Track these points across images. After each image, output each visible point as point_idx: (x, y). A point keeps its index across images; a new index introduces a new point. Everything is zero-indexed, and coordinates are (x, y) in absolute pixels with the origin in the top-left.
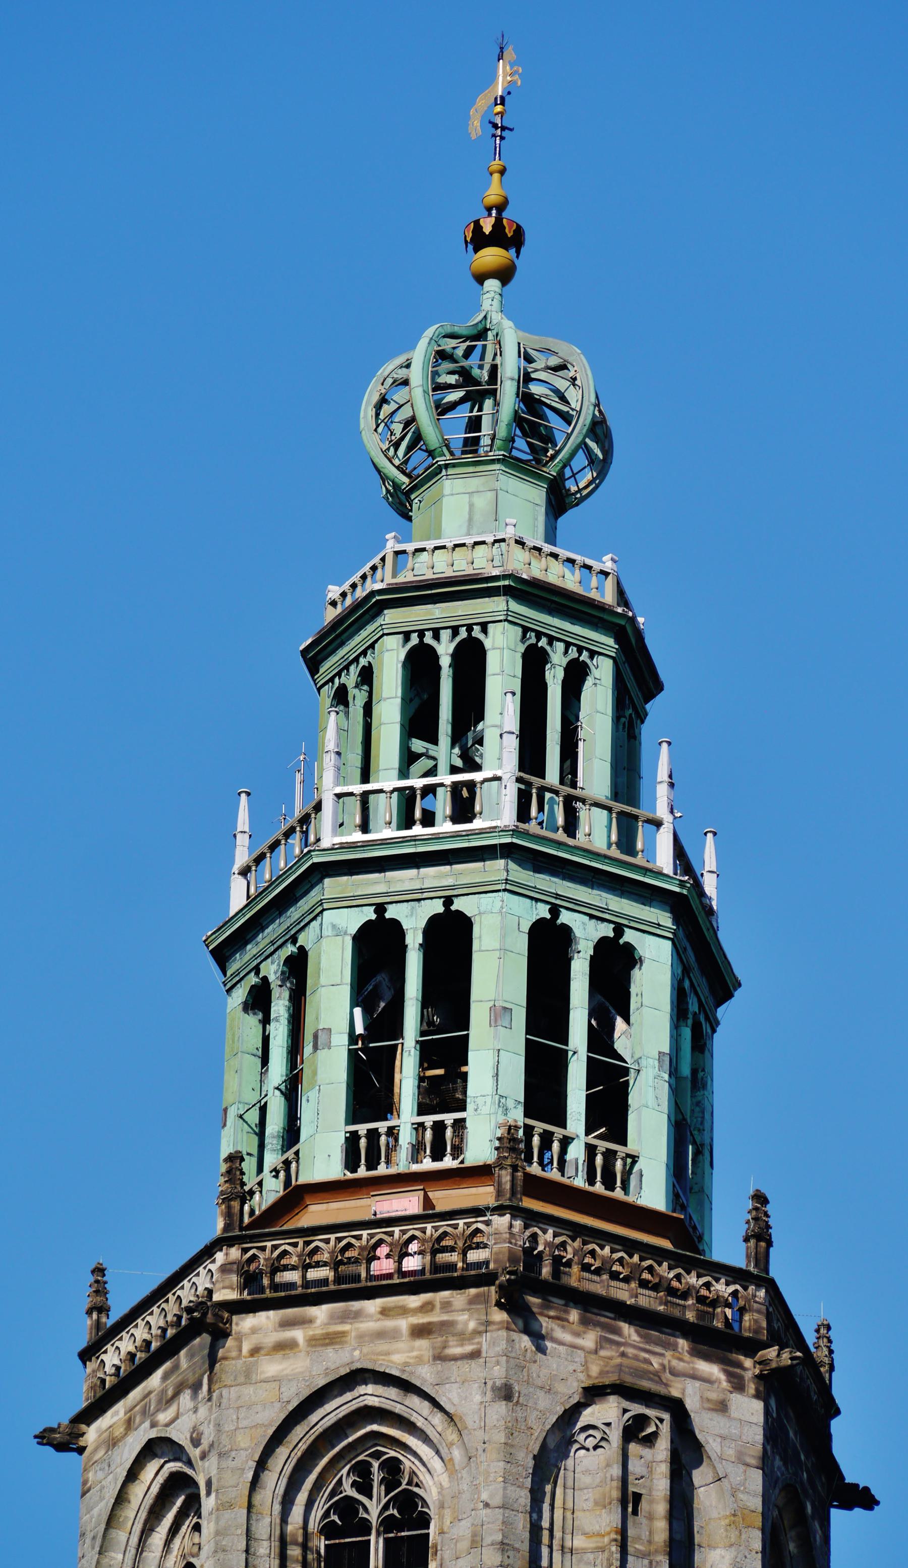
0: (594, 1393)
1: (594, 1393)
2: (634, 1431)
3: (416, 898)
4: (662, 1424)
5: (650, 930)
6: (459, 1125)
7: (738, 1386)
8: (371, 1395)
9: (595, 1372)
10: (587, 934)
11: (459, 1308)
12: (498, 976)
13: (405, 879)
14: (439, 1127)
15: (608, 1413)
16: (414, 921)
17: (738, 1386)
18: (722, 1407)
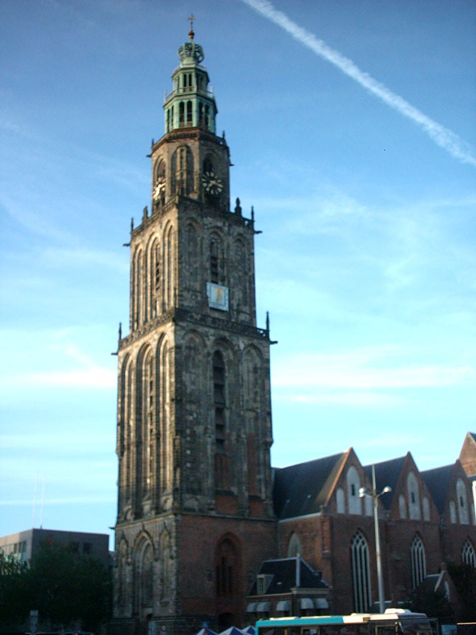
0: (177, 148)
1: (177, 148)
2: (182, 151)
3: (170, 106)
4: (184, 148)
5: (193, 98)
7: (195, 141)
8: (161, 157)
9: (179, 145)
10: (185, 101)
11: (165, 146)
12: (176, 110)
13: (169, 104)
15: (179, 150)
16: (170, 108)
17: (195, 141)
18: (193, 144)
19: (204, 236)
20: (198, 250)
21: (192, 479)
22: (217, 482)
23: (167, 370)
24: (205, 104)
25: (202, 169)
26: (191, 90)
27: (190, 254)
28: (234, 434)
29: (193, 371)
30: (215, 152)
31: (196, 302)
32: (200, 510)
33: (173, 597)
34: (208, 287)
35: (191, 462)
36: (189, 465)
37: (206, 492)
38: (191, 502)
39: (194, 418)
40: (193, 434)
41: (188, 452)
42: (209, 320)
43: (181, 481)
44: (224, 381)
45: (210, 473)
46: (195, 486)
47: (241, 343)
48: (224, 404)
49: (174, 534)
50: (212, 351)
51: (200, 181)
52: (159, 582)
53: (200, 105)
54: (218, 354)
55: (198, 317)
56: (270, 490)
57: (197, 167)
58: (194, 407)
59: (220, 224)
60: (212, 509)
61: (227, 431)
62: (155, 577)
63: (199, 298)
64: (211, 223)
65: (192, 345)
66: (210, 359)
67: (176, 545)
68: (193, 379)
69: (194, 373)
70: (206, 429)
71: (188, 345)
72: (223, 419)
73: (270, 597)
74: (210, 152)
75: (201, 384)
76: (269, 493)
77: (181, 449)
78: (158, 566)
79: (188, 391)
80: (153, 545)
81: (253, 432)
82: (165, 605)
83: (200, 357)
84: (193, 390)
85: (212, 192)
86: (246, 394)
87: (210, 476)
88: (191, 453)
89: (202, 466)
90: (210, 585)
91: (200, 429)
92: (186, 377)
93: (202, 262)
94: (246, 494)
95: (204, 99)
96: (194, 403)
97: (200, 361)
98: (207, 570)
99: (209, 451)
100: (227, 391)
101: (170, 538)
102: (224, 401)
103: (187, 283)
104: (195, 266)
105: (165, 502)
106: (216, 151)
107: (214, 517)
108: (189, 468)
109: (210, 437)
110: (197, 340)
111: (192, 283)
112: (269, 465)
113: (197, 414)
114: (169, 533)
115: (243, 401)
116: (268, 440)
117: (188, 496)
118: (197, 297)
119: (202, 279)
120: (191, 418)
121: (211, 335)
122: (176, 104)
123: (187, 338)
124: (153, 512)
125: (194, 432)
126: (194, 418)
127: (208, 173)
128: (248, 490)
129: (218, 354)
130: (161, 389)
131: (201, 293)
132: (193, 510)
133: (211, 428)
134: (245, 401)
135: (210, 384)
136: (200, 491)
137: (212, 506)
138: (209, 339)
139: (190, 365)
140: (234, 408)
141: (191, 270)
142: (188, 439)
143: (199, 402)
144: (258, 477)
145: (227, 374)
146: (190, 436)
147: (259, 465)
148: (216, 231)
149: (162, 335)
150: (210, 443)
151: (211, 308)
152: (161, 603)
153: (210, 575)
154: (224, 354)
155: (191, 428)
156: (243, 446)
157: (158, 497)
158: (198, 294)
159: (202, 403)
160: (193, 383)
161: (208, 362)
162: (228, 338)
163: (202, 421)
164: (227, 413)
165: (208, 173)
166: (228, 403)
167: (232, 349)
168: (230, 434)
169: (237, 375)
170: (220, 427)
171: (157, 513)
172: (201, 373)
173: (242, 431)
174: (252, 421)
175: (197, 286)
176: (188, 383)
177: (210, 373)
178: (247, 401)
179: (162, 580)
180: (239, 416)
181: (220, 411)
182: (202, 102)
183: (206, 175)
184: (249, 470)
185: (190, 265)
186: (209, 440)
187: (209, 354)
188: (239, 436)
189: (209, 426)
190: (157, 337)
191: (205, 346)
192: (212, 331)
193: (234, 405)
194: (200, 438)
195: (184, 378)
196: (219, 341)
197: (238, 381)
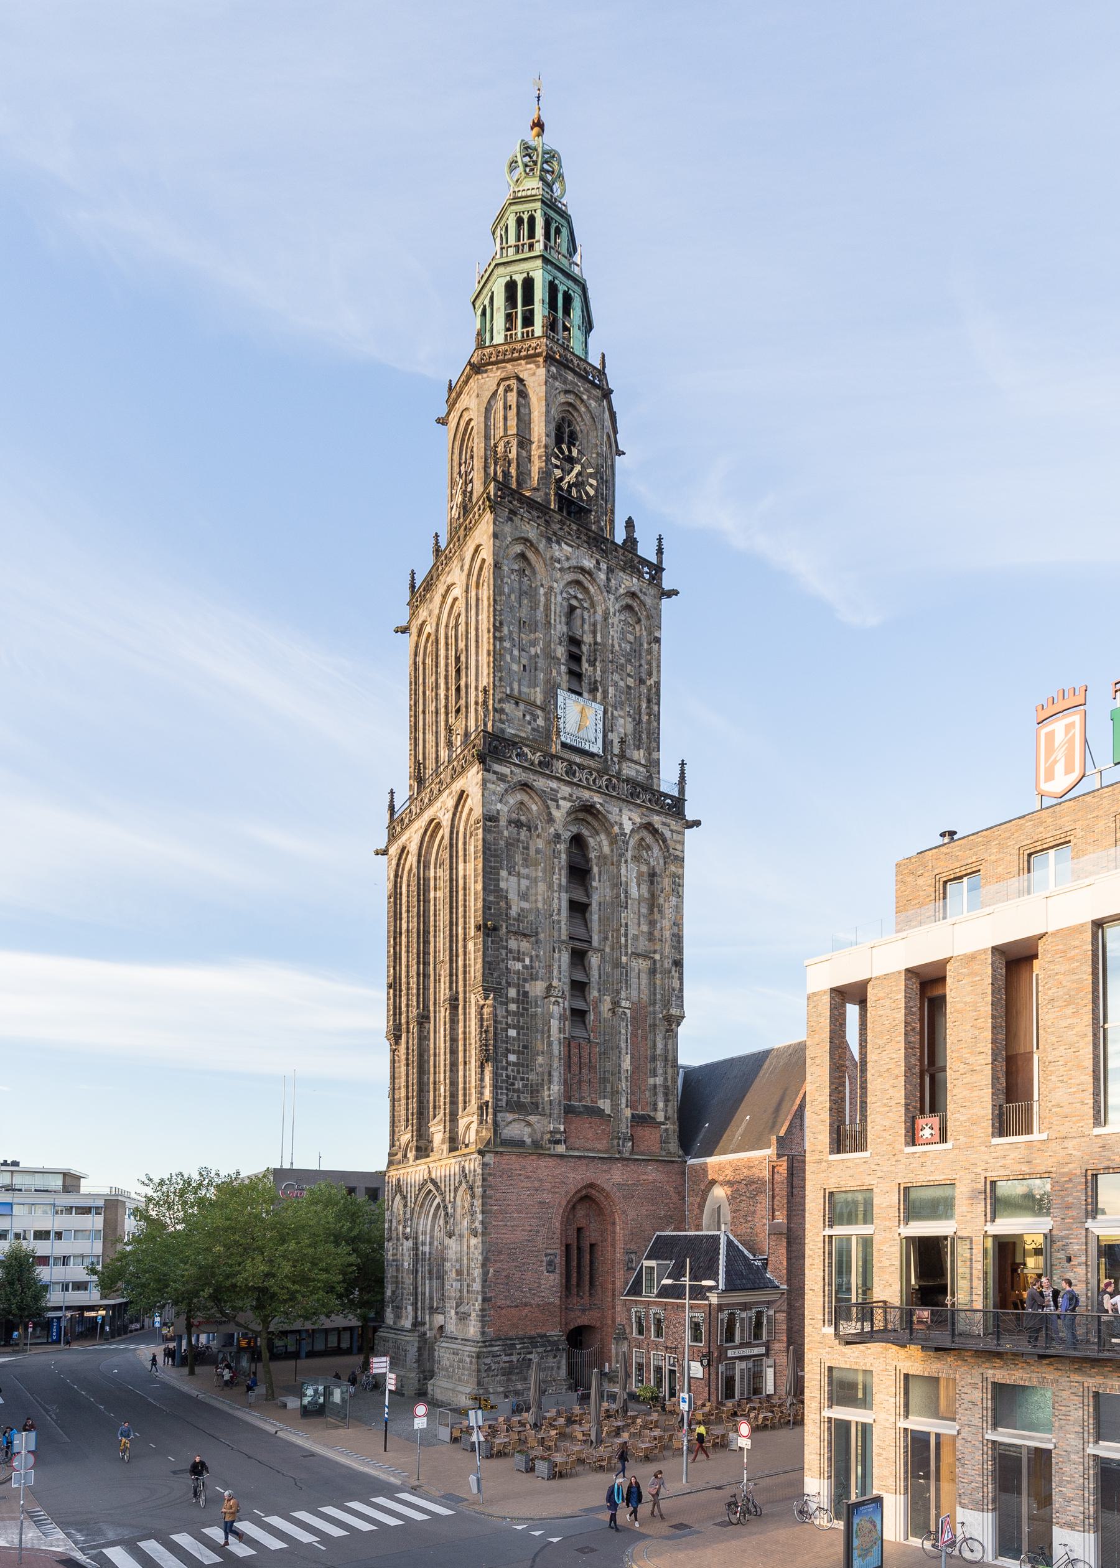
6: (533, 331)
14: (528, 332)
19: (553, 587)
20: (540, 615)
21: (519, 1084)
22: (568, 1094)
23: (471, 869)
24: (562, 288)
25: (553, 435)
26: (531, 246)
27: (521, 624)
28: (608, 998)
29: (524, 871)
30: (582, 401)
31: (533, 729)
32: (536, 1144)
33: (477, 1307)
34: (560, 699)
35: (518, 1053)
36: (512, 1058)
37: (547, 1107)
38: (516, 1129)
39: (525, 967)
40: (524, 998)
41: (512, 1033)
42: (559, 767)
43: (495, 1087)
44: (588, 896)
45: (555, 1074)
46: (526, 1098)
47: (627, 819)
48: (590, 942)
49: (479, 1191)
50: (567, 835)
51: (548, 461)
52: (453, 1275)
53: (553, 288)
54: (578, 841)
55: (537, 757)
56: (674, 1105)
57: (539, 430)
58: (525, 945)
59: (588, 564)
60: (558, 1142)
61: (595, 993)
62: (448, 1265)
63: (540, 722)
64: (568, 559)
65: (523, 818)
66: (562, 847)
67: (483, 1212)
68: (523, 888)
69: (527, 877)
70: (549, 987)
71: (514, 816)
72: (585, 970)
73: (666, 1304)
74: (571, 398)
75: (540, 898)
76: (673, 1111)
77: (496, 1028)
78: (452, 1244)
79: (513, 912)
80: (445, 1208)
81: (644, 997)
82: (463, 1317)
83: (540, 843)
84: (522, 910)
85: (574, 493)
86: (632, 921)
87: (556, 1079)
88: (518, 1034)
89: (540, 1060)
90: (550, 1283)
91: (537, 989)
92: (509, 883)
93: (547, 644)
94: (628, 1113)
95: (559, 275)
96: (525, 935)
97: (538, 851)
98: (546, 1255)
99: (554, 1031)
100: (594, 917)
101: (473, 1197)
102: (591, 937)
103: (516, 686)
104: (533, 651)
105: (468, 1127)
106: (585, 397)
107: (562, 1156)
108: (514, 1064)
109: (557, 1003)
110: (534, 808)
111: (525, 689)
112: (675, 1059)
113: (531, 957)
114: (471, 1188)
115: (626, 935)
116: (674, 1011)
117: (510, 1117)
118: (535, 718)
119: (548, 682)
120: (519, 966)
121: (564, 799)
122: (498, 288)
123: (512, 800)
124: (445, 1147)
125: (526, 994)
126: (525, 967)
127: (564, 447)
128: (632, 1105)
129: (578, 841)
130: (461, 909)
131: (543, 709)
132: (520, 1144)
133: (561, 983)
134: (630, 936)
135: (561, 902)
136: (535, 1108)
137: (558, 1136)
138: (558, 807)
139: (518, 858)
140: (608, 950)
141: (524, 661)
142: (513, 1007)
143: (537, 934)
144: (651, 1081)
145: (594, 884)
146: (516, 1001)
147: (654, 1059)
148: (580, 578)
149: (462, 796)
150: (557, 1016)
151: (564, 745)
152: (457, 1313)
153: (550, 1263)
154: (591, 840)
155: (518, 986)
156: (623, 1024)
157: (453, 1117)
158: (539, 712)
159: (542, 936)
160: (524, 897)
161: (556, 854)
162: (598, 806)
163: (541, 972)
164: (594, 960)
165: (564, 447)
166: (595, 942)
167: (608, 833)
168: (598, 1001)
169: (617, 883)
170: (579, 987)
171: (451, 1150)
172: (540, 874)
173: (623, 995)
174: (644, 976)
175: (538, 697)
176: (513, 896)
177: (560, 877)
178: (636, 938)
179: (459, 1273)
180: (617, 964)
181: (579, 957)
182: (557, 282)
183: (562, 452)
184: (636, 1068)
185: (521, 650)
186: (556, 1010)
187: (558, 836)
188: (616, 1004)
189: (555, 983)
190: (451, 803)
191: (551, 820)
192: (565, 790)
193: (608, 943)
194: (536, 1006)
195: (503, 885)
196: (581, 815)
197: (618, 896)
